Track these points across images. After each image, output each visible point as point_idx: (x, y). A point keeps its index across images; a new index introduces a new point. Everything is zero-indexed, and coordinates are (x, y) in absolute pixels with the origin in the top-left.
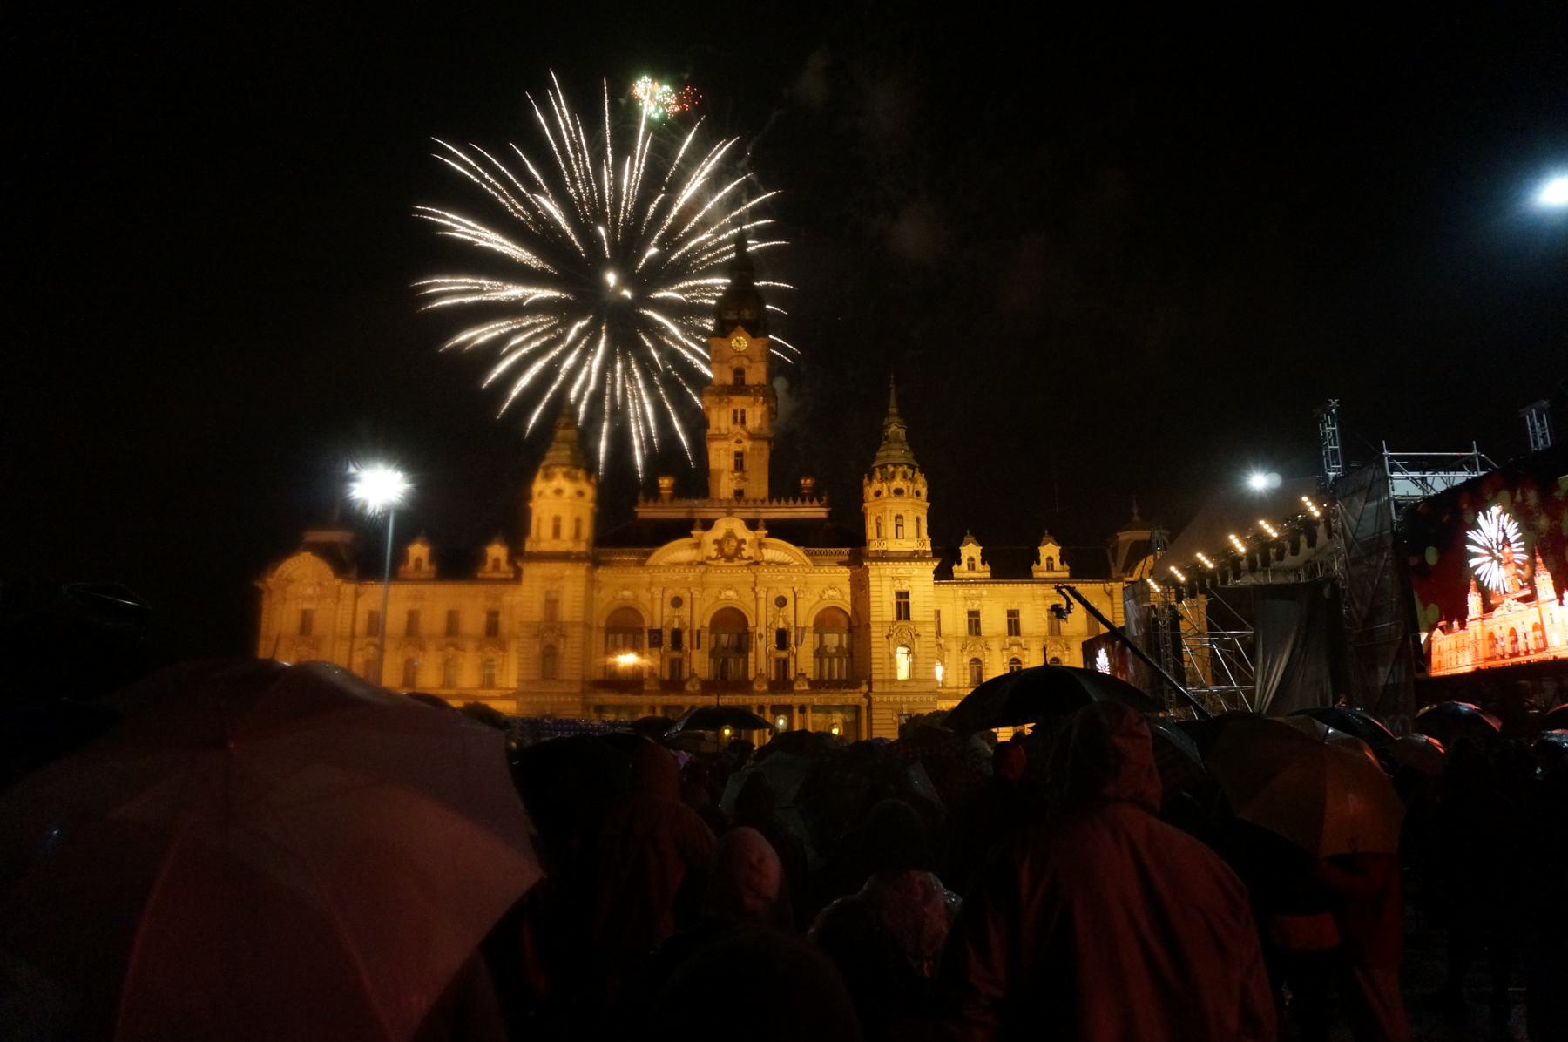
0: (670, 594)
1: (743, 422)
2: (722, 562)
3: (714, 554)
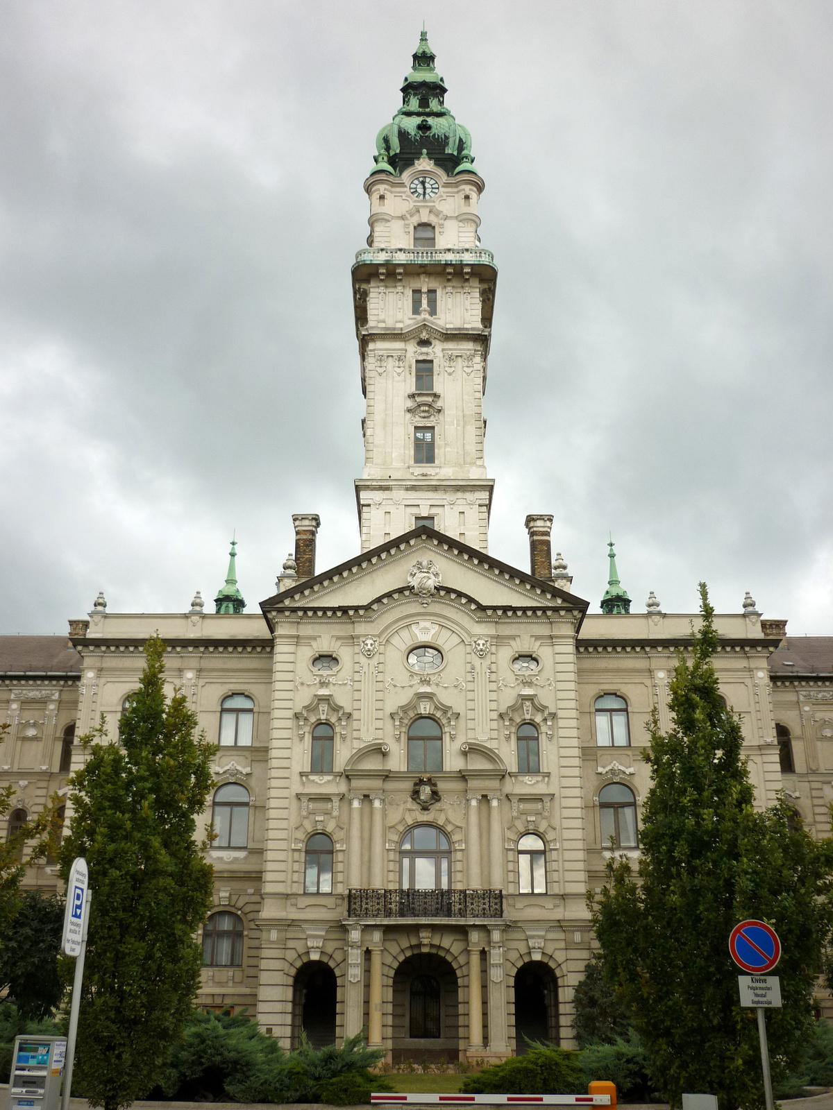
1: (433, 312)
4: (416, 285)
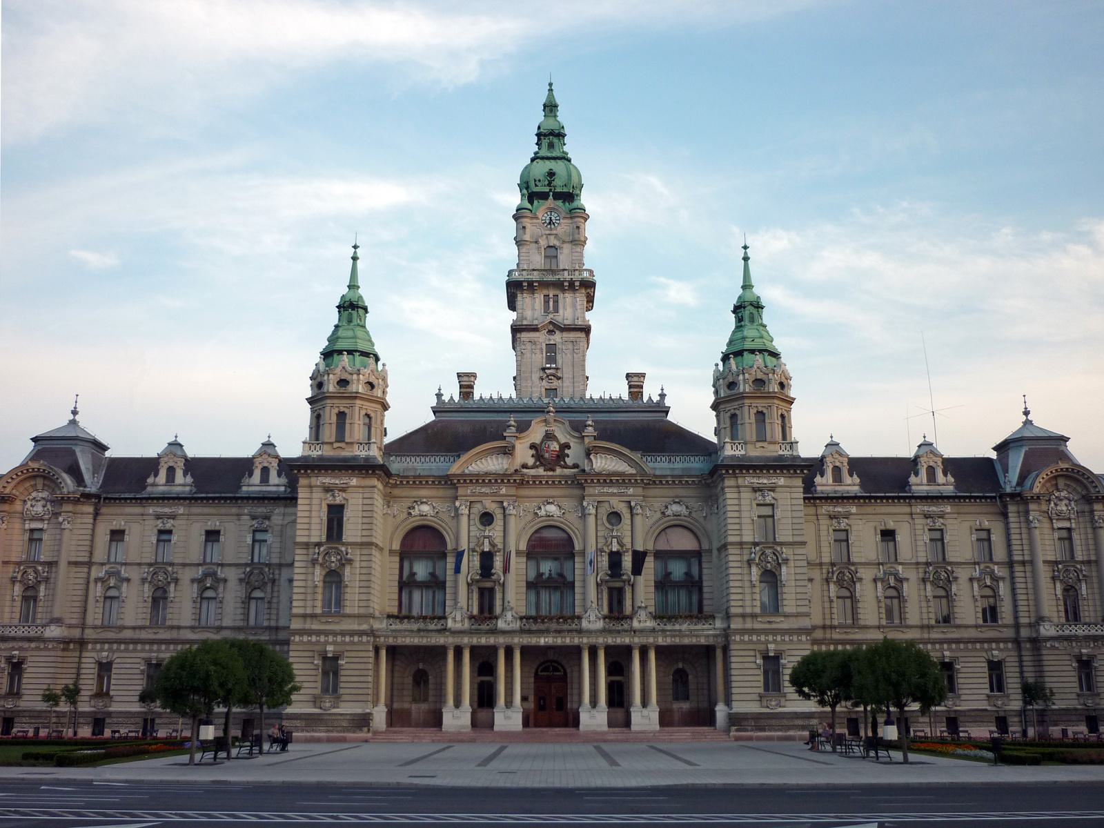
0: (477, 509)
1: (556, 310)
2: (541, 471)
3: (531, 461)
4: (546, 292)
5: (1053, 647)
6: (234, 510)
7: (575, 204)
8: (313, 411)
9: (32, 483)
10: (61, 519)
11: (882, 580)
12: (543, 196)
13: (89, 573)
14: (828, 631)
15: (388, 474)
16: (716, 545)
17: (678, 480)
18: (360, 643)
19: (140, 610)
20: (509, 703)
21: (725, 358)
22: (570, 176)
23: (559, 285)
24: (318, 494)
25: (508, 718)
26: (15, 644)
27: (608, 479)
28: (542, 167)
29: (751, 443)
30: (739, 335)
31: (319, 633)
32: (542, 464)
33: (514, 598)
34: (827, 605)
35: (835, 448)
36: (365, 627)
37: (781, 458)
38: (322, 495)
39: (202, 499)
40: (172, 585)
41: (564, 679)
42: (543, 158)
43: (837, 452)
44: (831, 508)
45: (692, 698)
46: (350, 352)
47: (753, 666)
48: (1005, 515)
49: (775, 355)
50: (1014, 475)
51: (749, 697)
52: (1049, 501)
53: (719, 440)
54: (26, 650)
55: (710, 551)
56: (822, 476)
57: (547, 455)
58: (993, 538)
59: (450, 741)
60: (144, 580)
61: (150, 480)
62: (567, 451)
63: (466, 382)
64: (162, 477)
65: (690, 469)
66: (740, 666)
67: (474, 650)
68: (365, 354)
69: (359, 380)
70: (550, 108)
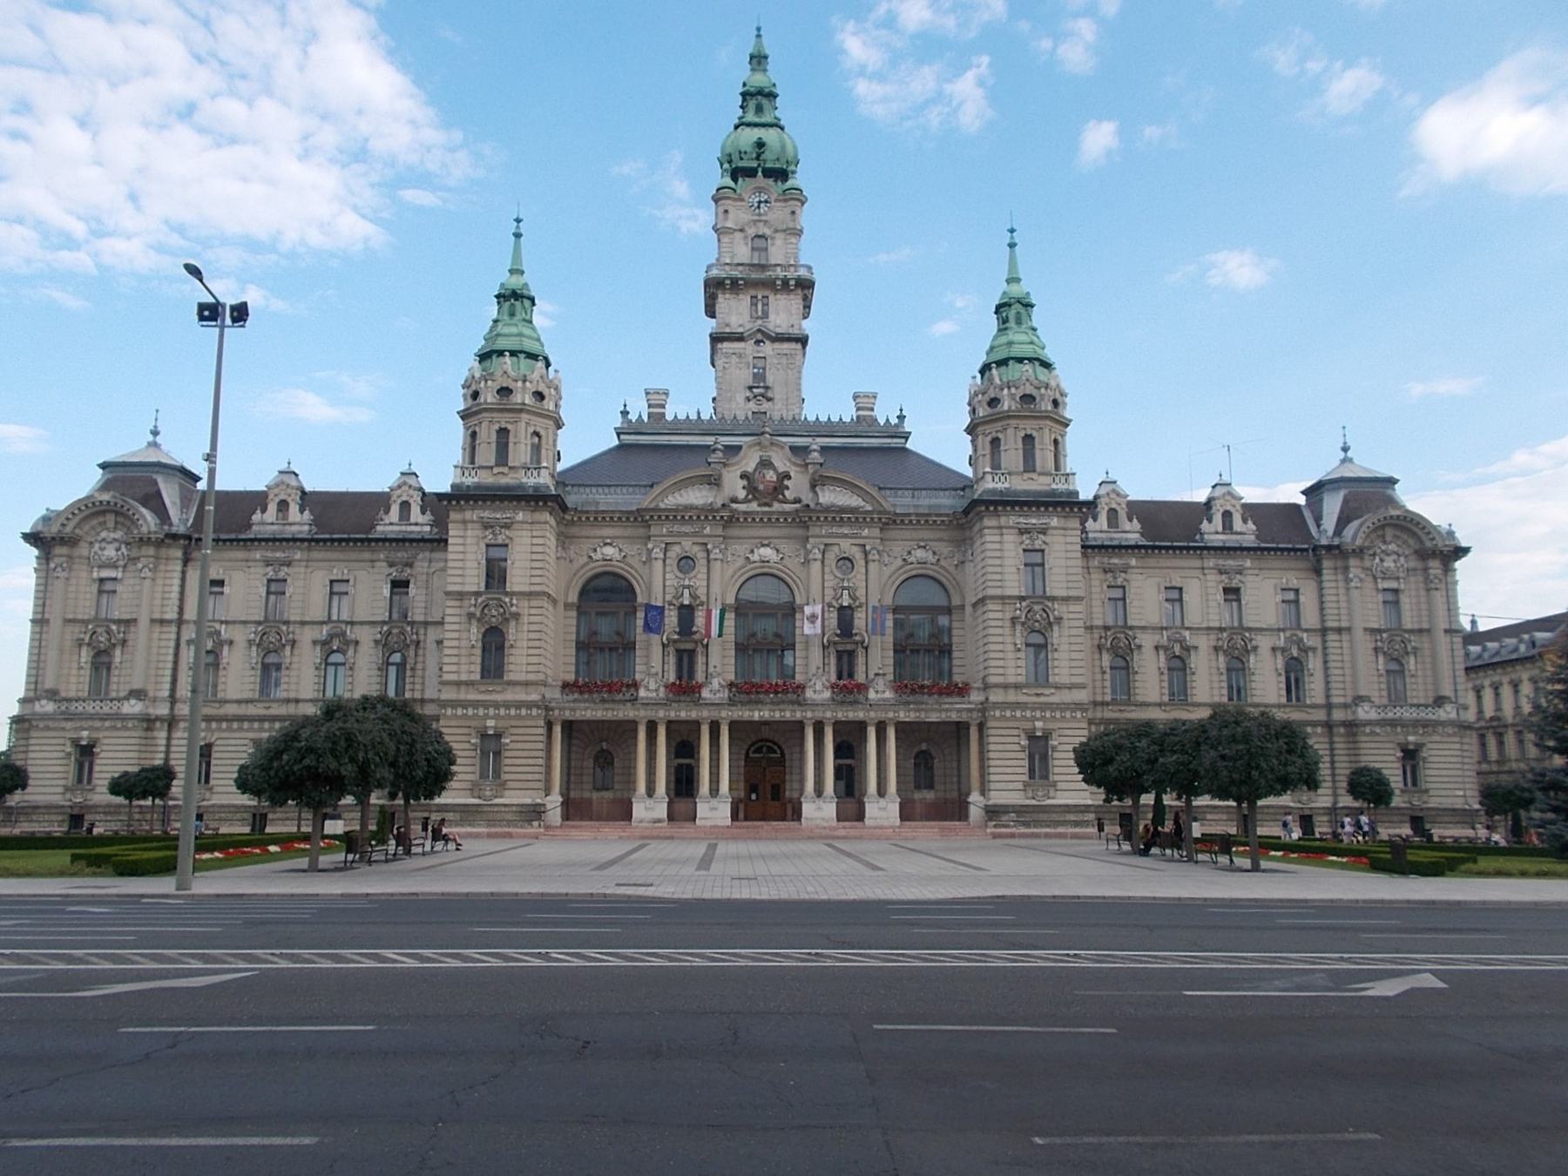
0: (675, 552)
1: (765, 315)
3: (742, 494)
4: (753, 292)
5: (1373, 733)
6: (367, 555)
7: (789, 184)
8: (467, 429)
9: (101, 519)
10: (140, 566)
11: (1166, 649)
12: (750, 173)
13: (178, 633)
14: (1099, 708)
15: (564, 508)
16: (971, 599)
17: (924, 520)
18: (529, 717)
19: (247, 680)
20: (714, 791)
21: (985, 369)
22: (783, 147)
23: (770, 285)
24: (473, 532)
25: (714, 810)
26: (84, 724)
27: (838, 515)
28: (749, 136)
29: (1017, 473)
30: (1003, 339)
31: (476, 704)
32: (755, 498)
33: (719, 666)
34: (1099, 676)
35: (1111, 487)
36: (534, 697)
37: (1053, 493)
38: (479, 533)
39: (325, 541)
40: (288, 648)
41: (781, 762)
42: (749, 125)
43: (1114, 491)
44: (1106, 560)
45: (937, 786)
46: (513, 353)
47: (1017, 747)
48: (1318, 572)
49: (1047, 365)
50: (1329, 523)
51: (1011, 786)
52: (1374, 555)
53: (975, 472)
54: (97, 729)
55: (962, 607)
56: (1095, 520)
57: (761, 487)
58: (1302, 599)
59: (643, 838)
60: (250, 642)
61: (257, 517)
62: (786, 482)
63: (657, 399)
64: (271, 513)
65: (939, 506)
66: (1000, 747)
67: (670, 723)
68: (533, 356)
69: (524, 388)
70: (758, 60)
